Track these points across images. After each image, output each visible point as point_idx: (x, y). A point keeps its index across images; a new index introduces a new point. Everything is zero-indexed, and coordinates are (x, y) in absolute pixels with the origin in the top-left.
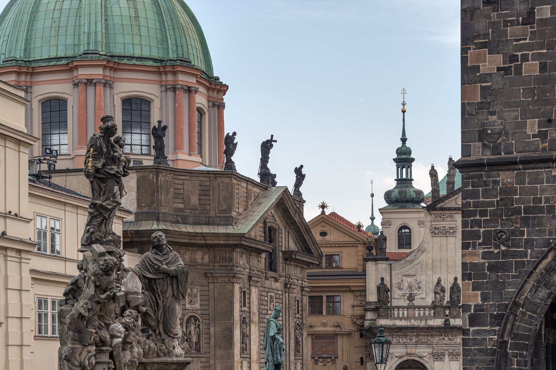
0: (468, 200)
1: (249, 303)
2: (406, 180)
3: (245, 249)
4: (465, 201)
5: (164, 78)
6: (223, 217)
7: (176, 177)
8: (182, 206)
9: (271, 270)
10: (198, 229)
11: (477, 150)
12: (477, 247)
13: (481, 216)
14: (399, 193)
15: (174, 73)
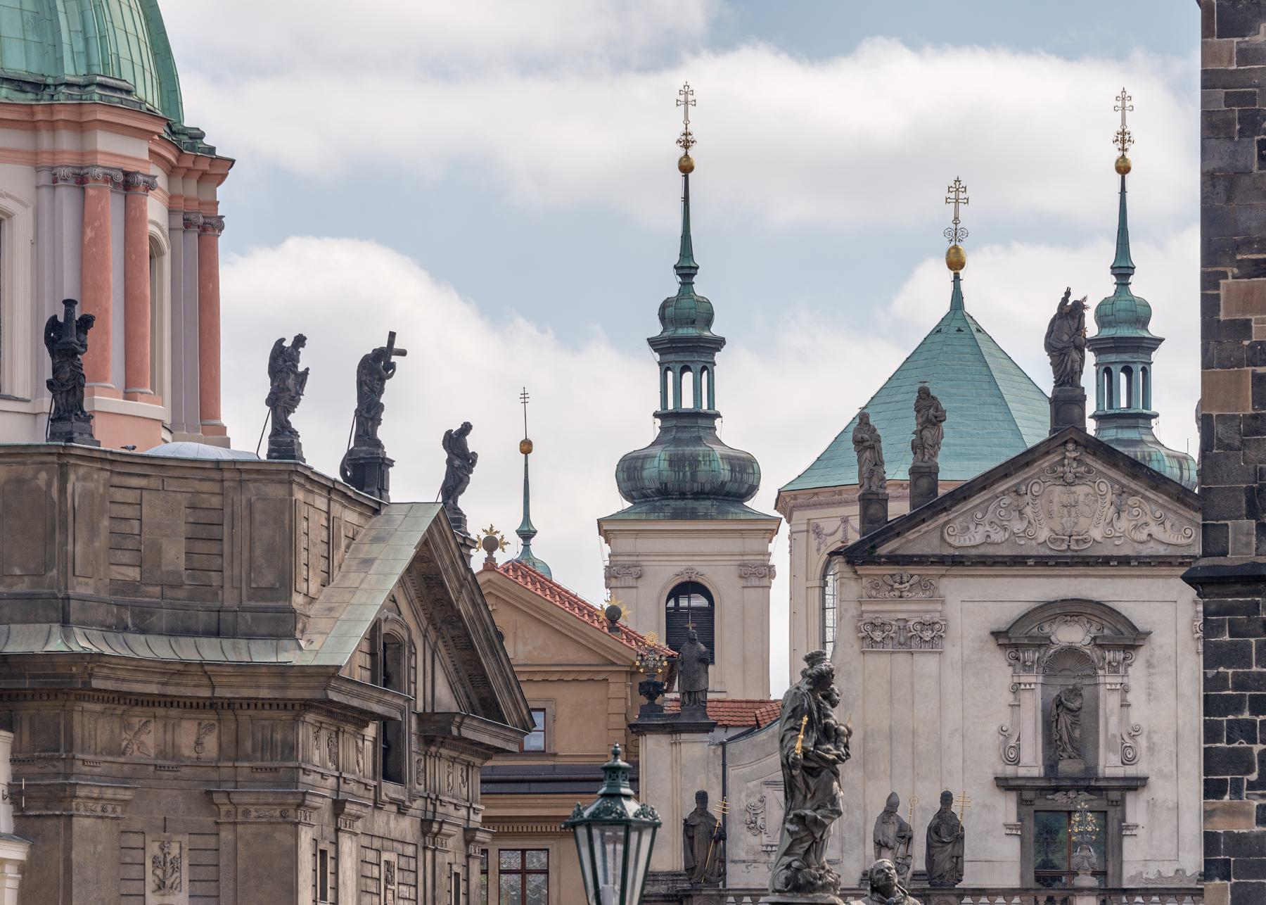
0: (1221, 669)
1: (336, 889)
2: (694, 415)
3: (330, 714)
4: (1212, 673)
5: (45, 141)
6: (265, 610)
7: (117, 480)
8: (133, 574)
9: (387, 776)
10: (188, 650)
11: (1244, 539)
12: (1245, 792)
13: (1255, 712)
14: (672, 462)
15: (81, 127)
